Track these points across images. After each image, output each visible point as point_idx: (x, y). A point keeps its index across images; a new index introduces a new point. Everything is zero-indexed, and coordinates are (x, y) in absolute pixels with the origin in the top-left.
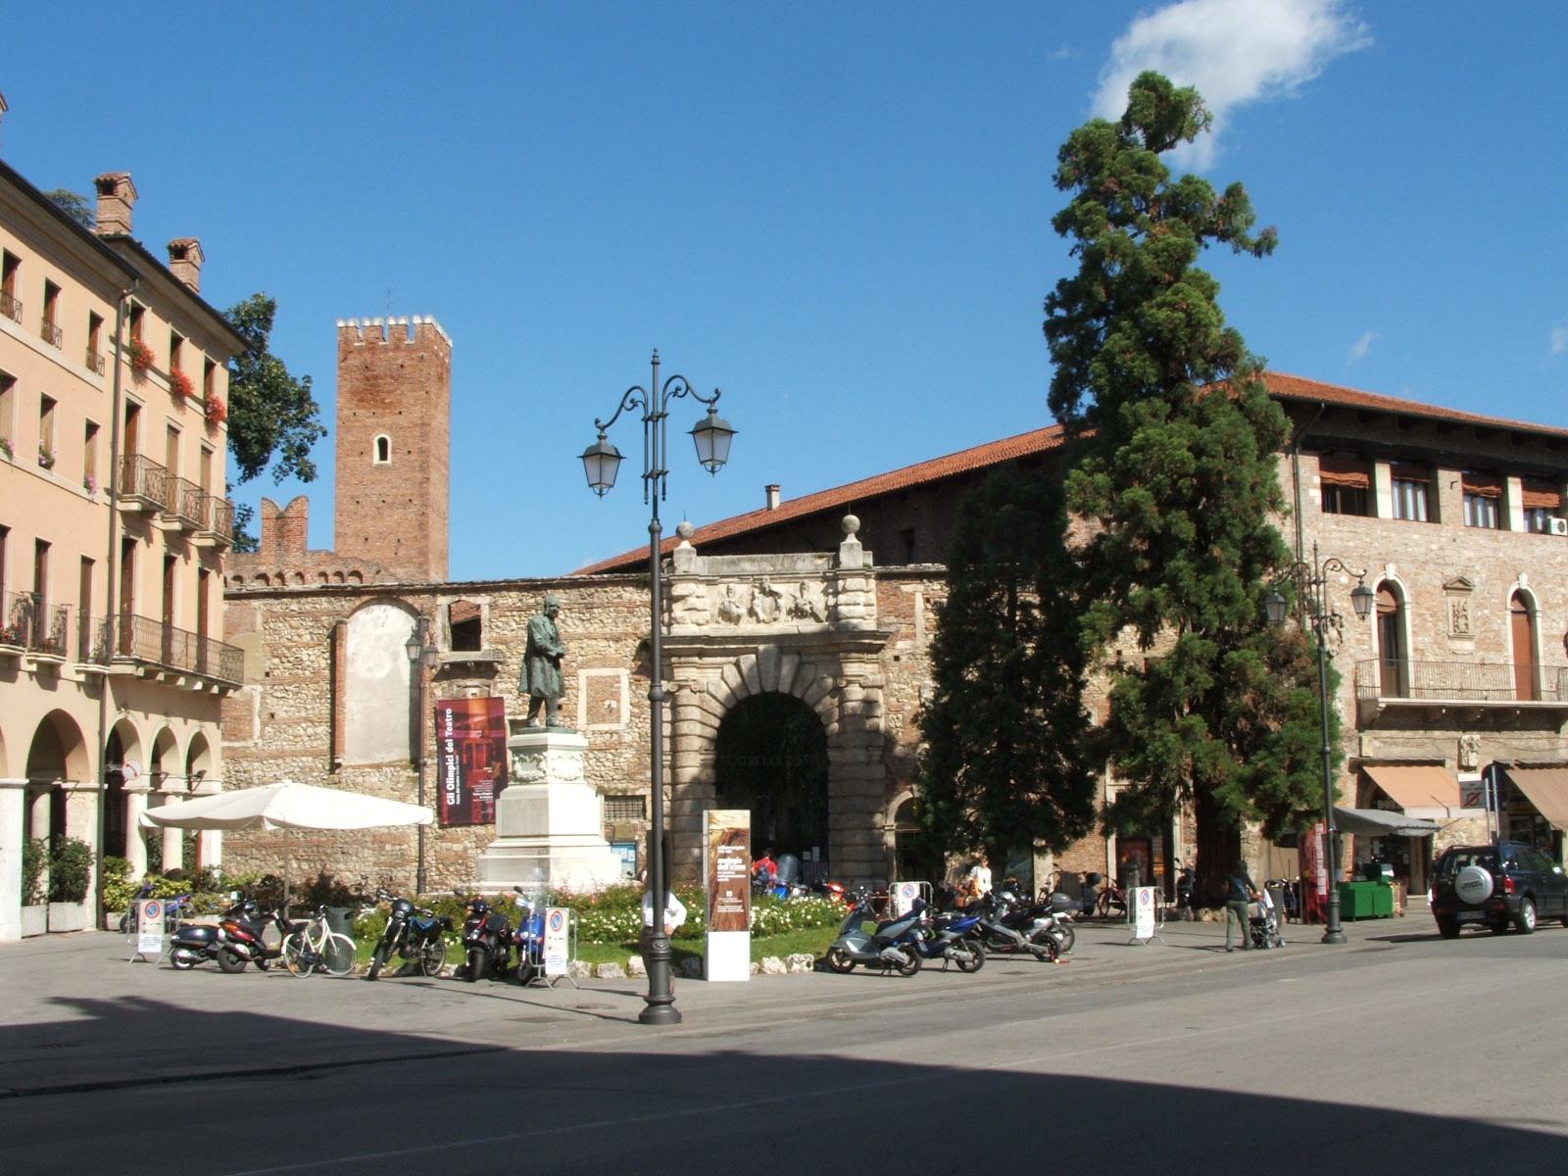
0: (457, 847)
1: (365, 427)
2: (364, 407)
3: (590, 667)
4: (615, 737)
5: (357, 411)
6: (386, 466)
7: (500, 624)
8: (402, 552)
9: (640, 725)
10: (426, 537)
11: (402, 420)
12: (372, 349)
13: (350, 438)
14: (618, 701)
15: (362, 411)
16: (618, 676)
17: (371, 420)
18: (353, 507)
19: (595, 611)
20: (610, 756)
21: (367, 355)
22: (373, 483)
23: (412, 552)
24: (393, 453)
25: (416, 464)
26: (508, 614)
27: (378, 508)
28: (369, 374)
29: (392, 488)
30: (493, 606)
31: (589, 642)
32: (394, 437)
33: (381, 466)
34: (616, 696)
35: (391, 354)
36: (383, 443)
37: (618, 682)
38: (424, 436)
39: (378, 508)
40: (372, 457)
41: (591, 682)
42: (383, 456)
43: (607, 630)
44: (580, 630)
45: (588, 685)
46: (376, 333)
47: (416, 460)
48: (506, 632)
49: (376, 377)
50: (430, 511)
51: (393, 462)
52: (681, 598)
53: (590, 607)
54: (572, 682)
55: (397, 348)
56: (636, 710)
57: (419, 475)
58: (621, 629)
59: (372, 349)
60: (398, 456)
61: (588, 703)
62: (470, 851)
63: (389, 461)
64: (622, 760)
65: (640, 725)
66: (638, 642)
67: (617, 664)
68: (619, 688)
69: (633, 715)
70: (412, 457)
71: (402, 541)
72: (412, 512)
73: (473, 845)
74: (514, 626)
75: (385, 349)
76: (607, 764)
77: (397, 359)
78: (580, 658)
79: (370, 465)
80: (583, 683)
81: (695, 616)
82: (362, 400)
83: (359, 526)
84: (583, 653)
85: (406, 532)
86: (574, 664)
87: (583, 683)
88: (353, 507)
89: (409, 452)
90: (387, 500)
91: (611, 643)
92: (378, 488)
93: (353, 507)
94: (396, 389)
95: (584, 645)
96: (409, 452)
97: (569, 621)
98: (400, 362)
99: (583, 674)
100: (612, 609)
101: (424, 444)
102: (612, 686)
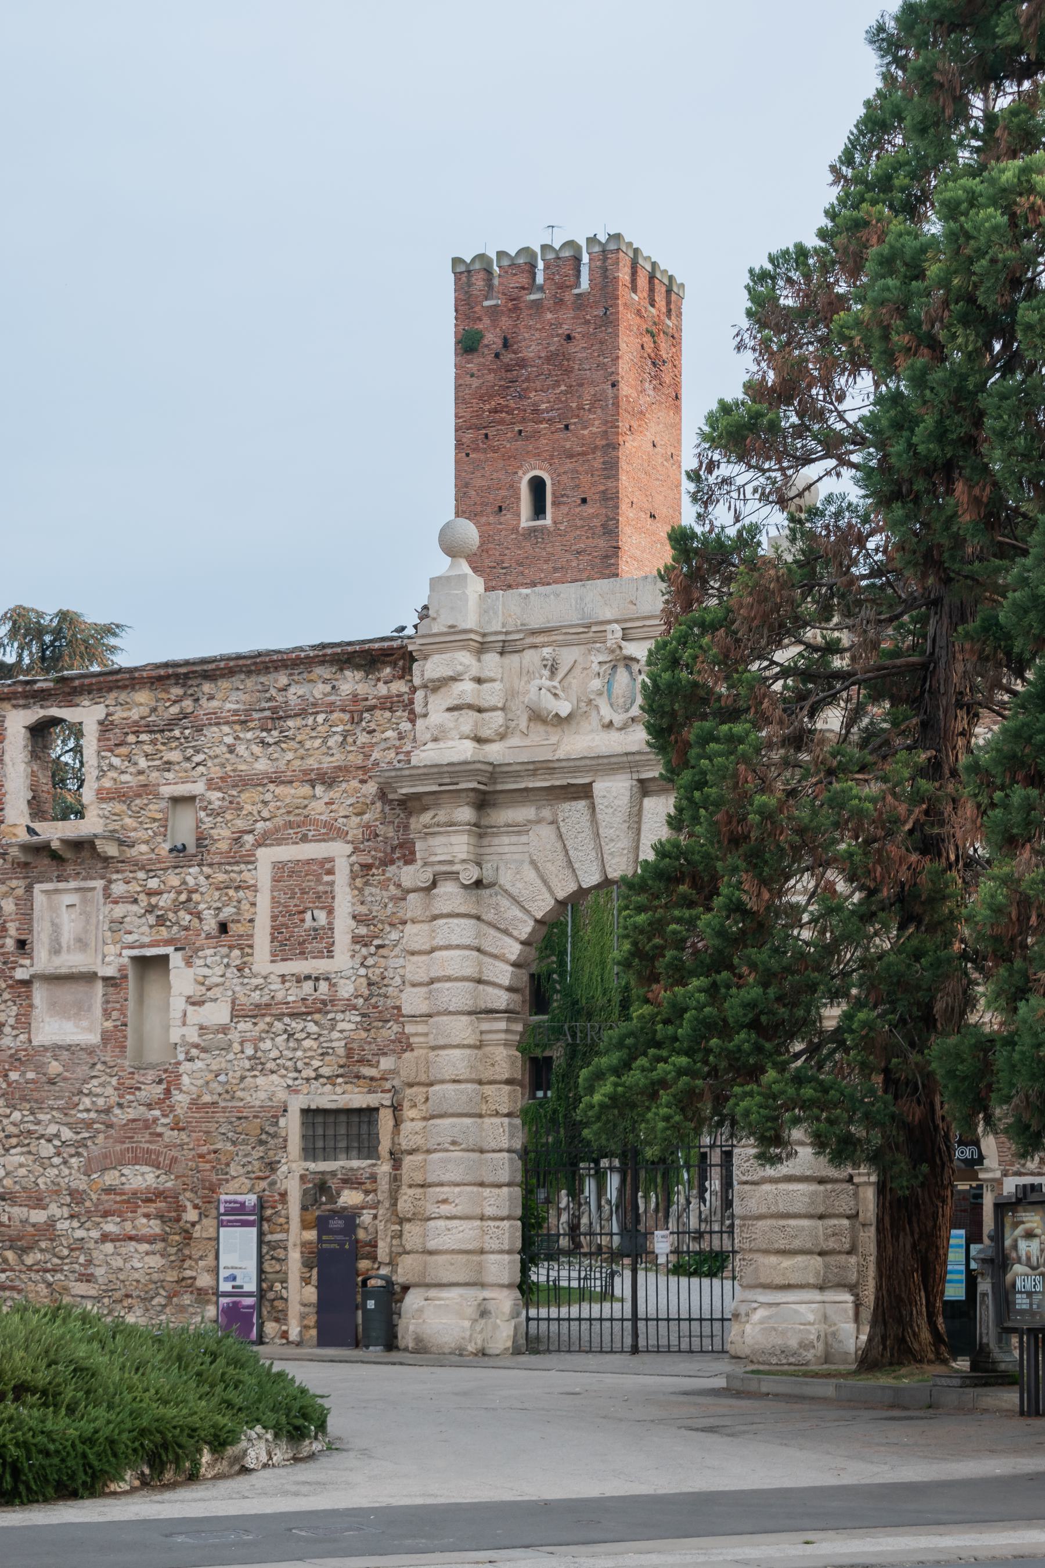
0: (38, 1216)
3: (279, 842)
4: (323, 986)
6: (543, 529)
7: (116, 761)
9: (370, 961)
12: (516, 308)
13: (479, 482)
14: (330, 912)
16: (331, 860)
19: (290, 723)
20: (312, 1028)
21: (505, 322)
22: (521, 564)
24: (554, 503)
25: (597, 522)
26: (131, 738)
28: (508, 357)
29: (555, 570)
30: (105, 726)
31: (280, 790)
32: (557, 475)
33: (533, 530)
34: (325, 900)
35: (549, 316)
36: (538, 486)
37: (331, 872)
38: (611, 468)
40: (519, 515)
41: (282, 872)
42: (539, 510)
43: (311, 763)
44: (262, 765)
45: (276, 880)
48: (125, 778)
49: (522, 364)
51: (555, 523)
52: (437, 686)
53: (277, 716)
54: (246, 875)
56: (363, 931)
57: (602, 543)
58: (338, 758)
59: (516, 308)
60: (564, 509)
61: (274, 918)
62: (59, 1226)
63: (548, 521)
64: (335, 1035)
65: (370, 961)
66: (371, 788)
67: (331, 832)
68: (332, 884)
69: (357, 940)
70: (589, 510)
73: (66, 1212)
74: (143, 763)
75: (537, 304)
76: (307, 1043)
78: (260, 825)
79: (515, 530)
80: (262, 875)
81: (467, 721)
84: (265, 814)
86: (249, 839)
87: (262, 875)
89: (584, 501)
91: (319, 790)
94: (557, 384)
95: (268, 797)
96: (584, 501)
97: (241, 749)
98: (565, 329)
99: (267, 856)
100: (320, 718)
101: (610, 484)
102: (319, 881)
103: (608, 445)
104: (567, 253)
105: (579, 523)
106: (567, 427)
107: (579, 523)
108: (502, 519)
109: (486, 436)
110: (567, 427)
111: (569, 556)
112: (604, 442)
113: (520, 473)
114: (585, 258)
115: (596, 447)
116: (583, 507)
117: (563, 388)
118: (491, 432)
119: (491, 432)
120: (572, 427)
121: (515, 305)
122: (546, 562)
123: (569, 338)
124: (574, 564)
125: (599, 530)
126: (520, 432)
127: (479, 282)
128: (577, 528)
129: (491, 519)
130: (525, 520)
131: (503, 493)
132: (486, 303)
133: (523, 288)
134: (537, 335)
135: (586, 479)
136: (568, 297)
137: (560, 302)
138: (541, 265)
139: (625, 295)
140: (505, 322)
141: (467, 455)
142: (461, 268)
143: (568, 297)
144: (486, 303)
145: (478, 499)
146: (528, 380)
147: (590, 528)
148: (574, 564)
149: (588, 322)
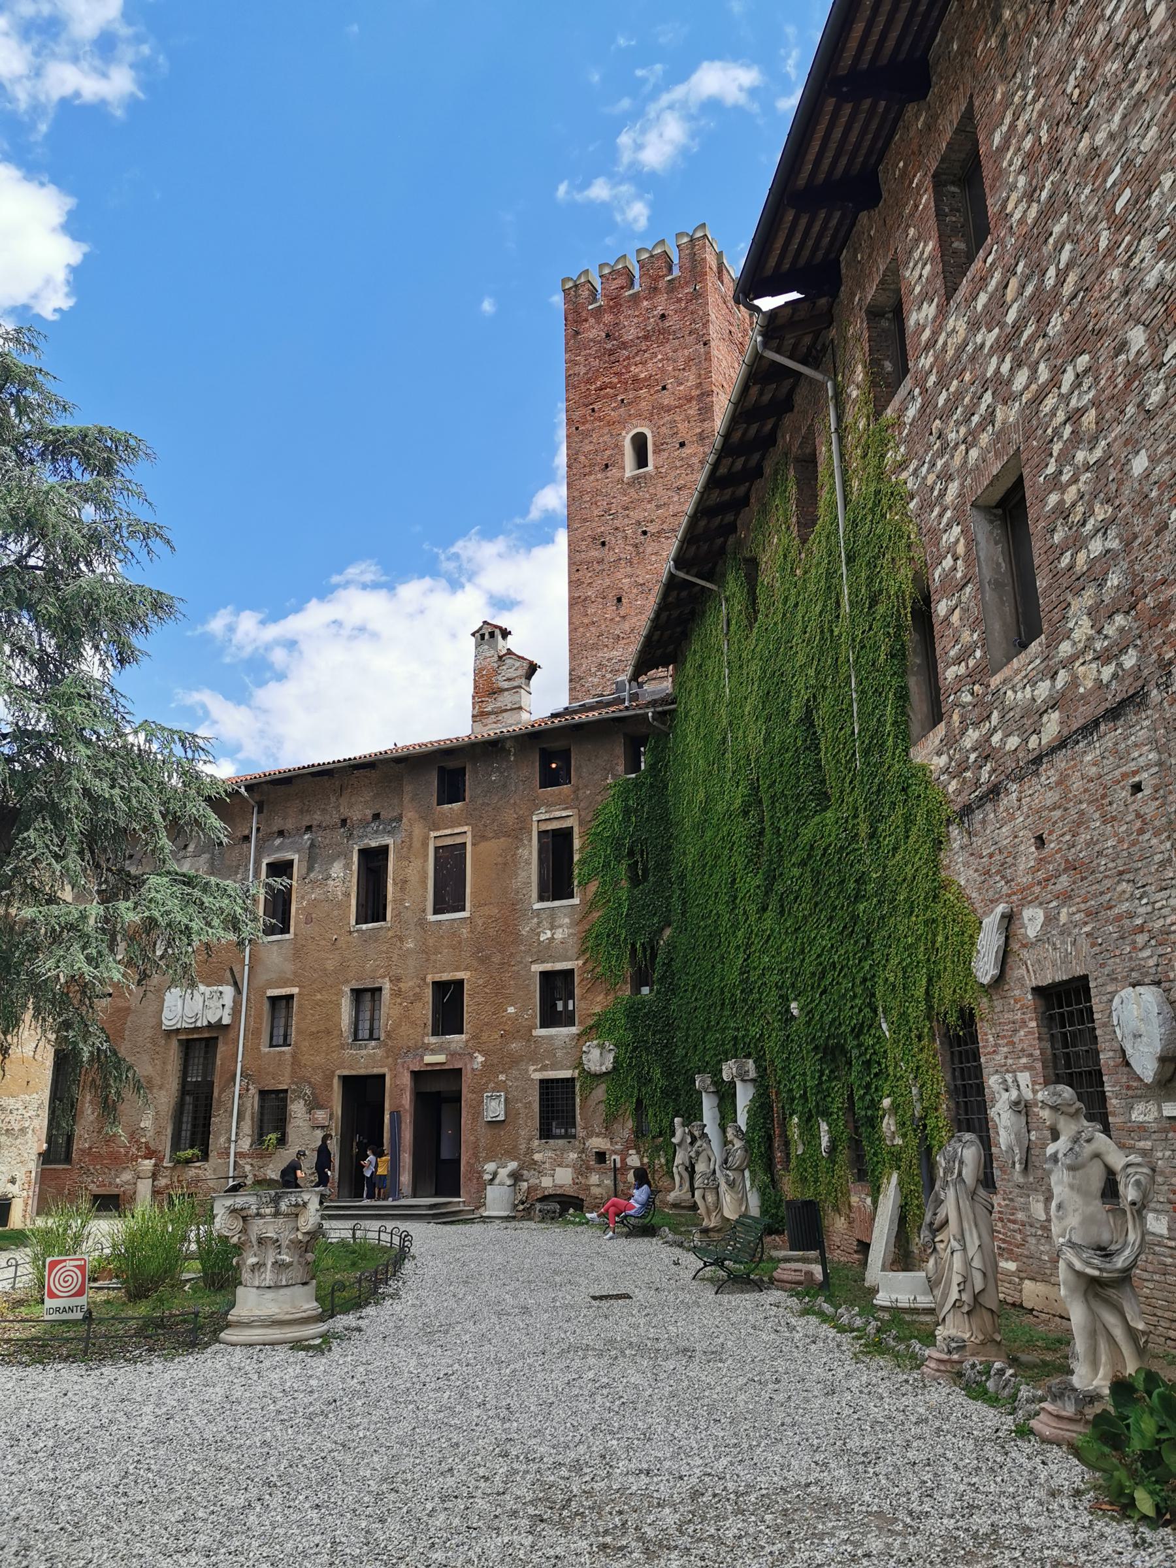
21: (608, 318)
22: (627, 509)
24: (654, 452)
25: (695, 460)
27: (636, 546)
29: (658, 507)
33: (636, 478)
35: (645, 303)
36: (640, 443)
39: (636, 546)
40: (623, 468)
42: (642, 461)
46: (621, 281)
49: (624, 345)
60: (666, 454)
63: (650, 467)
70: (687, 451)
75: (635, 298)
83: (607, 582)
88: (595, 554)
90: (652, 528)
92: (636, 515)
94: (655, 355)
96: (682, 445)
98: (659, 311)
101: (706, 425)
103: (702, 394)
105: (678, 464)
106: (664, 388)
107: (678, 464)
108: (609, 474)
109: (593, 410)
111: (670, 493)
112: (698, 392)
113: (624, 433)
114: (676, 261)
115: (692, 398)
117: (660, 357)
118: (595, 406)
119: (595, 406)
120: (669, 386)
121: (615, 303)
122: (649, 502)
123: (663, 316)
124: (675, 499)
126: (622, 400)
129: (599, 476)
131: (608, 453)
132: (590, 307)
133: (622, 288)
134: (635, 320)
135: (682, 427)
137: (654, 290)
139: (711, 279)
140: (608, 318)
141: (577, 429)
142: (570, 285)
143: (662, 284)
144: (590, 307)
145: (587, 463)
146: (628, 358)
147: (690, 466)
148: (675, 499)
149: (679, 300)
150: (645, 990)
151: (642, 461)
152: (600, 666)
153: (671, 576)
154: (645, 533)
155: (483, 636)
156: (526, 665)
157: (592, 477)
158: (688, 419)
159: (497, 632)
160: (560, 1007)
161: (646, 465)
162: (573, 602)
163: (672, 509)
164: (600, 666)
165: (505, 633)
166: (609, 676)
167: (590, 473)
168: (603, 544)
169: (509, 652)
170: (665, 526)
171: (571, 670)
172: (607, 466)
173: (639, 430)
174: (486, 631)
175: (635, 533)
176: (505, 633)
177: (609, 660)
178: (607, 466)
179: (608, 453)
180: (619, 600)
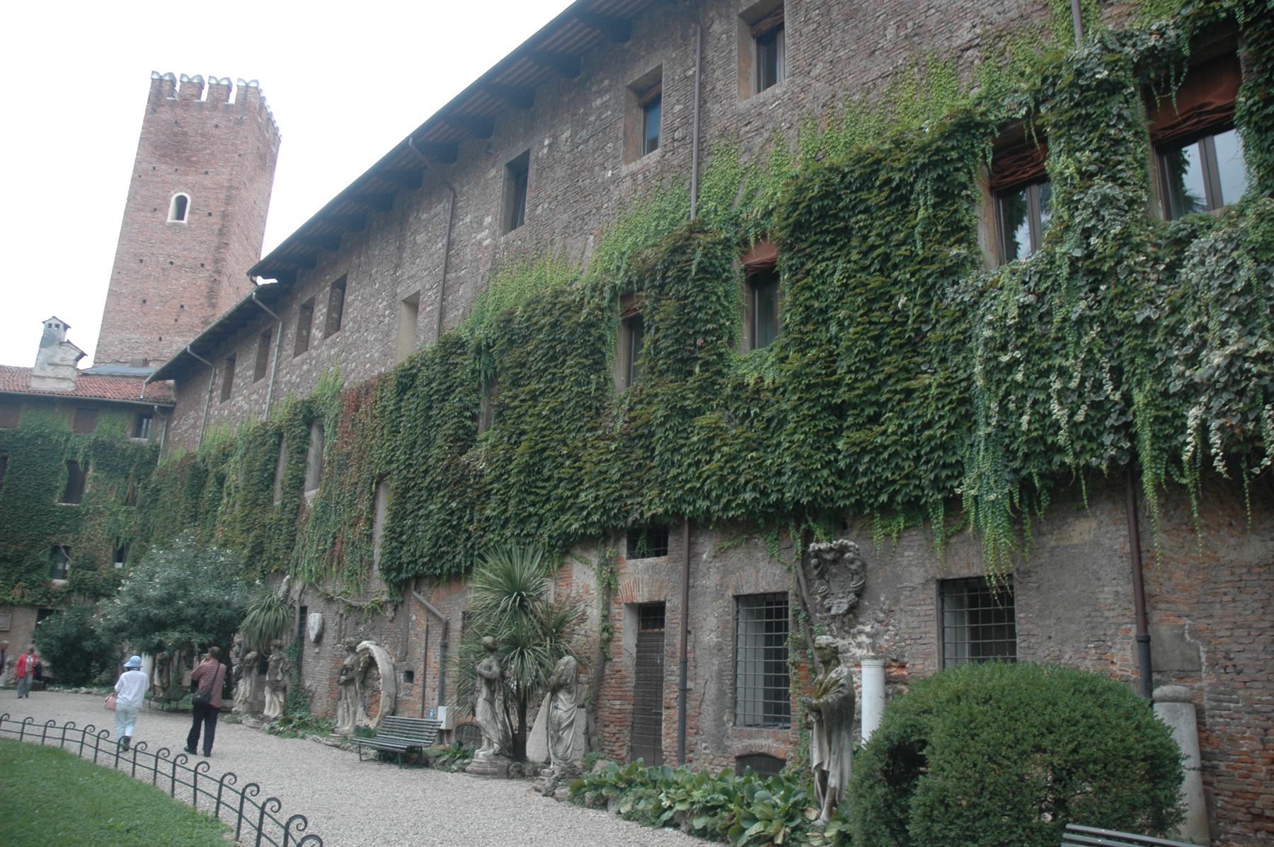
1: (163, 182)
2: (166, 163)
5: (157, 166)
6: (180, 226)
8: (184, 319)
10: (213, 306)
11: (207, 181)
15: (163, 167)
17: (171, 176)
18: (133, 265)
23: (196, 321)
24: (190, 212)
25: (216, 227)
27: (164, 270)
29: (185, 249)
33: (175, 225)
36: (181, 202)
38: (229, 200)
39: (164, 270)
42: (180, 215)
46: (194, 91)
47: (214, 224)
49: (185, 134)
50: (224, 279)
51: (189, 223)
55: (215, 108)
60: (197, 217)
63: (185, 222)
70: (212, 220)
71: (186, 308)
72: (202, 277)
77: (213, 119)
79: (163, 223)
82: (164, 156)
85: (191, 298)
89: (210, 214)
93: (133, 265)
96: (210, 214)
98: (215, 121)
104: (225, 82)
107: (205, 226)
110: (206, 173)
116: (210, 218)
122: (180, 244)
125: (217, 232)
127: (167, 87)
128: (202, 228)
129: (149, 214)
130: (170, 219)
131: (159, 201)
136: (221, 105)
138: (207, 87)
142: (155, 77)
149: (230, 120)
150: (119, 565)
151: (180, 215)
152: (121, 342)
153: (185, 352)
154: (172, 263)
155: (50, 325)
156: (78, 354)
157: (143, 214)
158: (217, 199)
159: (61, 326)
160: (60, 566)
161: (182, 219)
162: (111, 293)
163: (194, 254)
164: (121, 342)
165: (66, 327)
166: (126, 349)
167: (142, 210)
168: (141, 261)
169: (68, 342)
170: (186, 264)
171: (100, 338)
172: (155, 209)
173: (180, 194)
174: (54, 322)
175: (165, 261)
176: (66, 327)
177: (129, 339)
178: (155, 209)
179: (159, 201)
180: (144, 301)
